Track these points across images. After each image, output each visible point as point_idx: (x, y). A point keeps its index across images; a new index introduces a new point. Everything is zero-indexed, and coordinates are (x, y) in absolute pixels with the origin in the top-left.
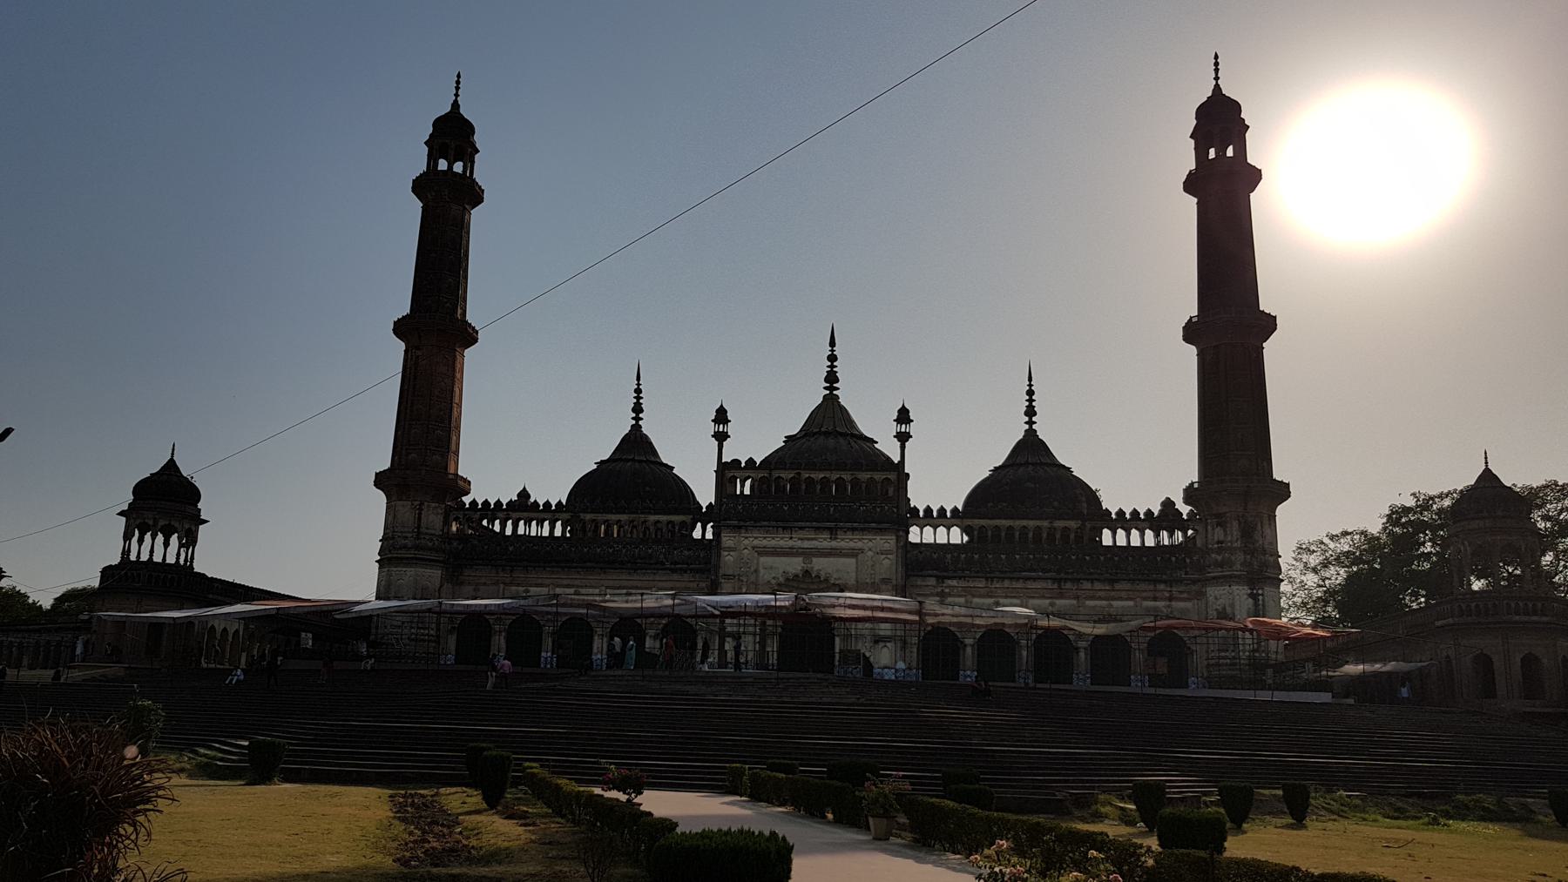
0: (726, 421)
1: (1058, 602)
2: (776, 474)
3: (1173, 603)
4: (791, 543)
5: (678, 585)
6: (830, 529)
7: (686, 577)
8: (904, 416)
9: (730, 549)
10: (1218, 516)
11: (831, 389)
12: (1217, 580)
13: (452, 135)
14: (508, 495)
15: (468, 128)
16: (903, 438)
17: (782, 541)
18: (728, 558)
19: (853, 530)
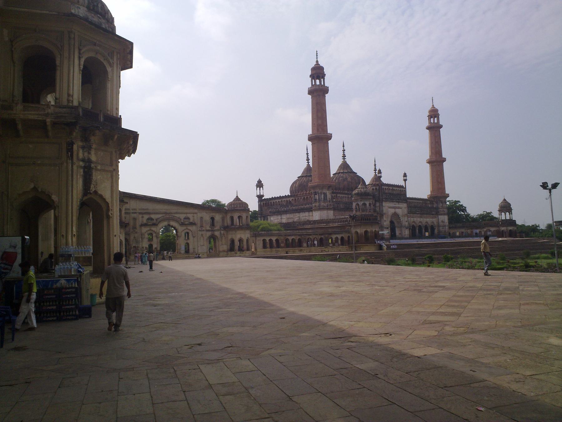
0: (381, 173)
6: (399, 202)
8: (405, 175)
11: (344, 159)
12: (441, 214)
16: (405, 180)
17: (392, 204)
18: (385, 210)
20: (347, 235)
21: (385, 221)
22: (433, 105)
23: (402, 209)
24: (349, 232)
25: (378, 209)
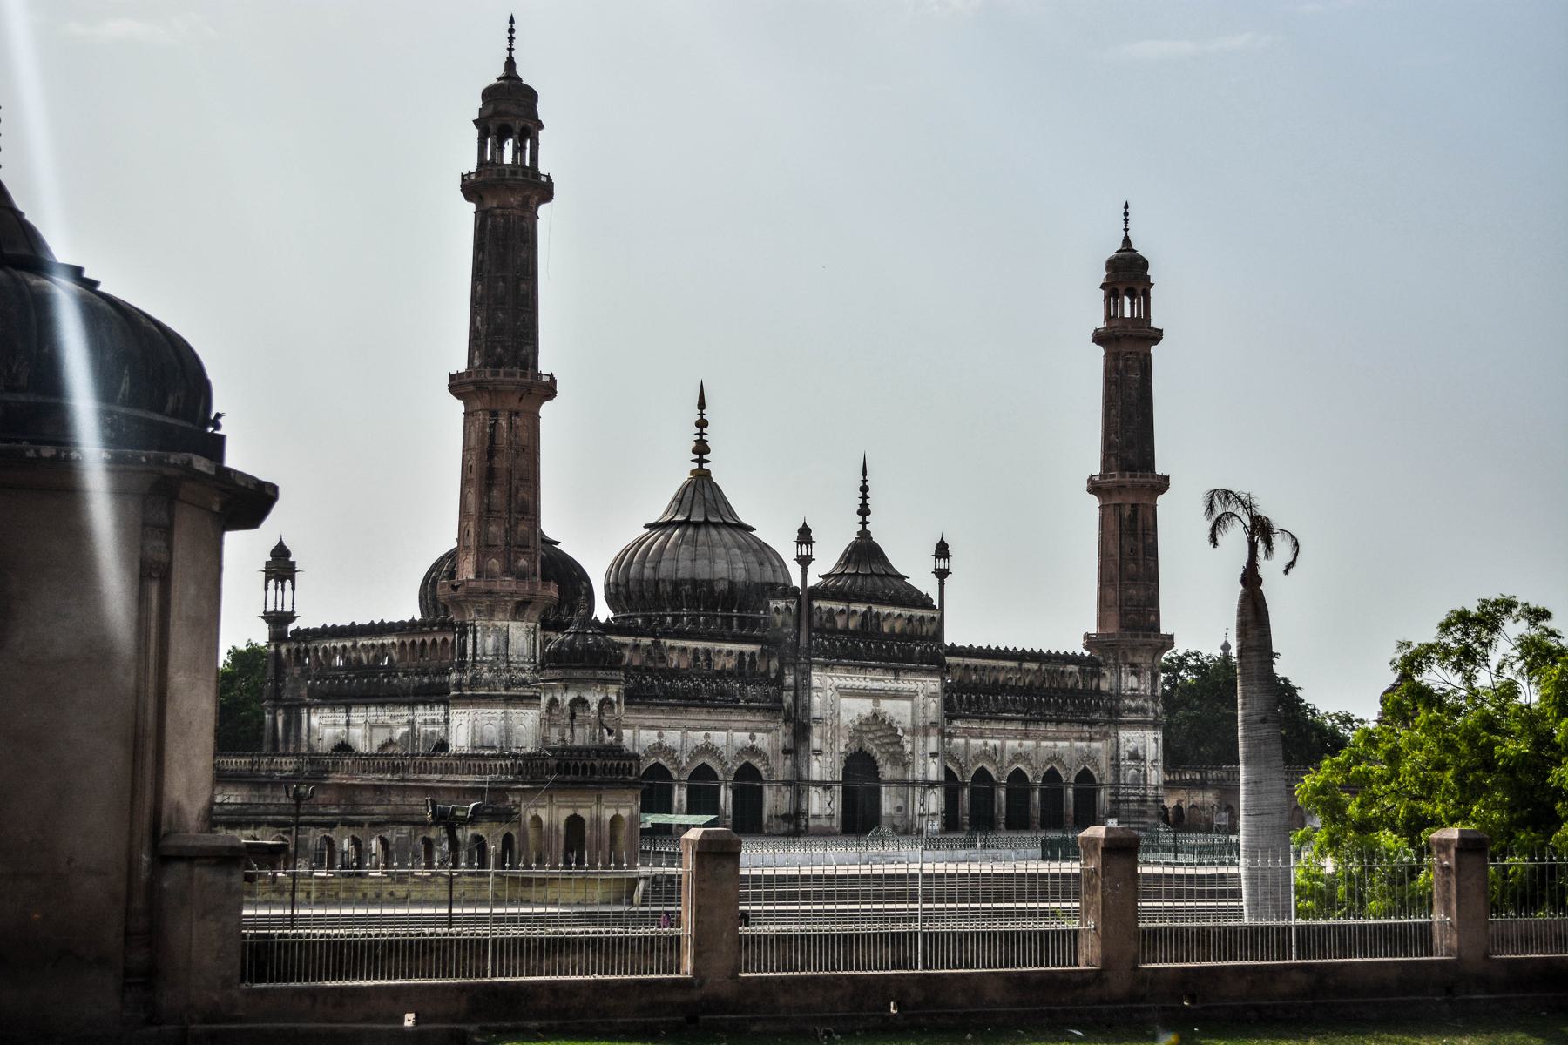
1: (1025, 743)
2: (852, 607)
3: (1095, 745)
4: (863, 684)
5: (750, 725)
6: (896, 671)
7: (759, 717)
8: (942, 551)
9: (820, 690)
10: (1133, 665)
11: (701, 461)
12: (1132, 725)
13: (509, 109)
16: (942, 574)
19: (912, 670)
20: (501, 830)
21: (820, 752)
22: (1127, 240)
23: (911, 699)
24: (506, 816)
25: (788, 698)
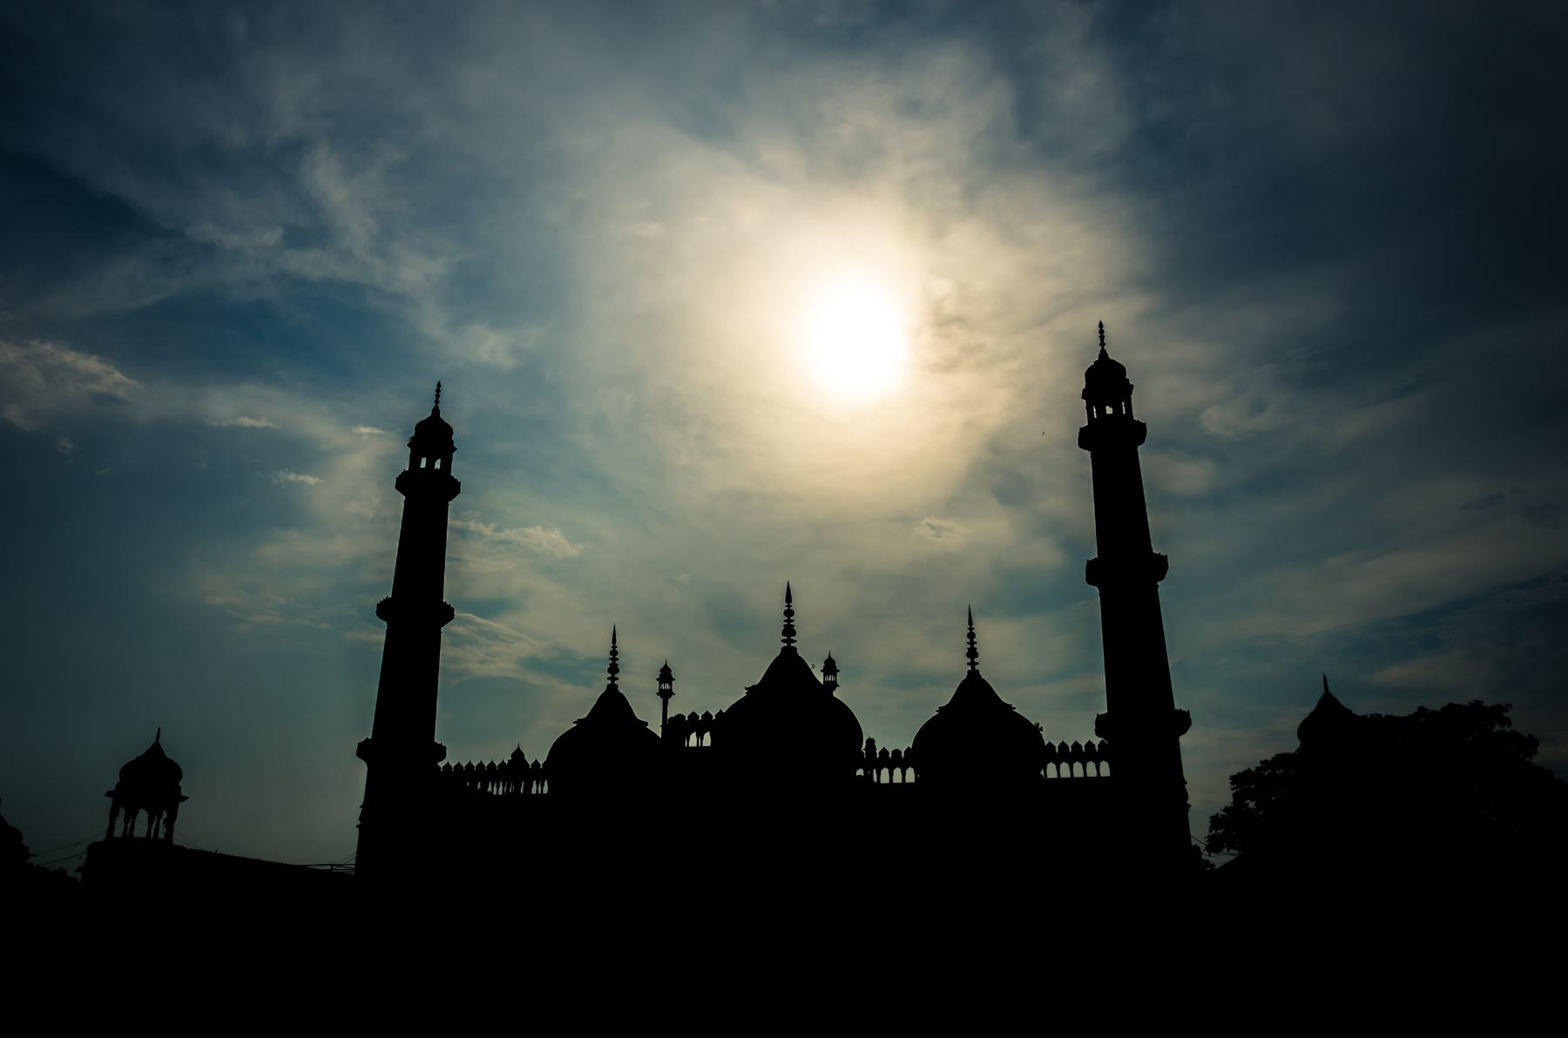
8: (830, 667)
14: (502, 756)
15: (448, 430)
22: (1103, 354)
